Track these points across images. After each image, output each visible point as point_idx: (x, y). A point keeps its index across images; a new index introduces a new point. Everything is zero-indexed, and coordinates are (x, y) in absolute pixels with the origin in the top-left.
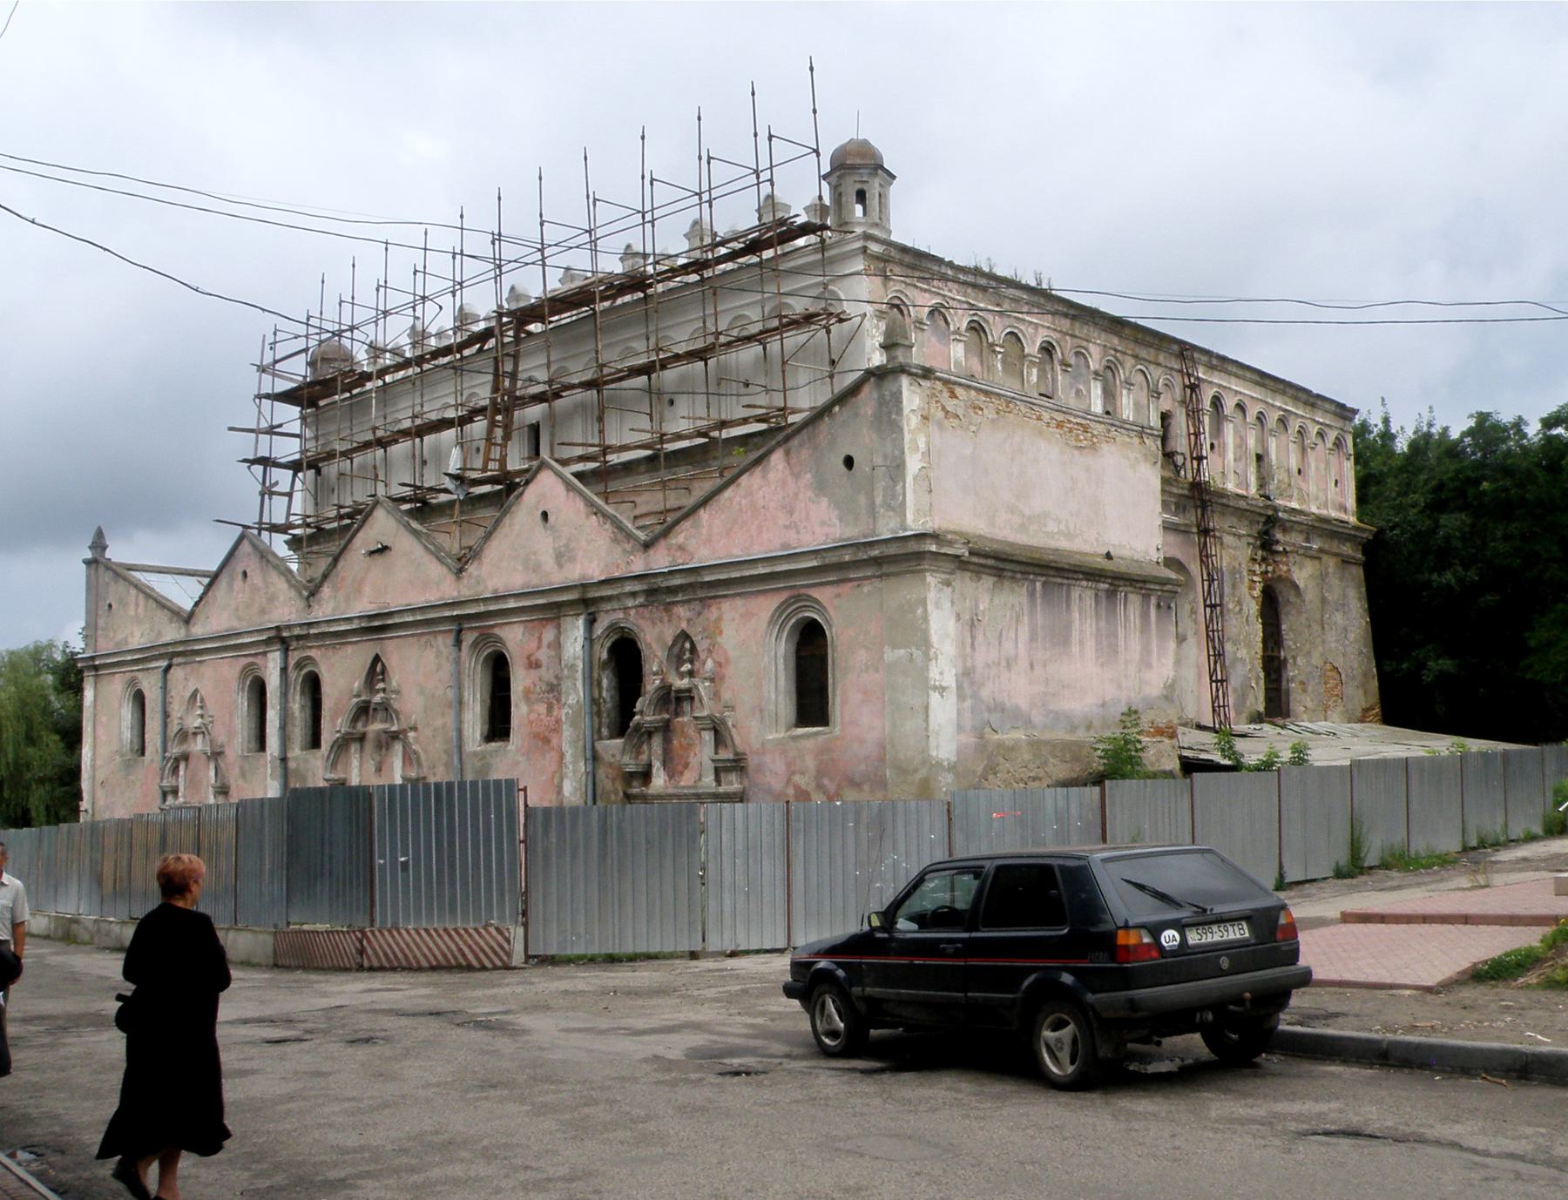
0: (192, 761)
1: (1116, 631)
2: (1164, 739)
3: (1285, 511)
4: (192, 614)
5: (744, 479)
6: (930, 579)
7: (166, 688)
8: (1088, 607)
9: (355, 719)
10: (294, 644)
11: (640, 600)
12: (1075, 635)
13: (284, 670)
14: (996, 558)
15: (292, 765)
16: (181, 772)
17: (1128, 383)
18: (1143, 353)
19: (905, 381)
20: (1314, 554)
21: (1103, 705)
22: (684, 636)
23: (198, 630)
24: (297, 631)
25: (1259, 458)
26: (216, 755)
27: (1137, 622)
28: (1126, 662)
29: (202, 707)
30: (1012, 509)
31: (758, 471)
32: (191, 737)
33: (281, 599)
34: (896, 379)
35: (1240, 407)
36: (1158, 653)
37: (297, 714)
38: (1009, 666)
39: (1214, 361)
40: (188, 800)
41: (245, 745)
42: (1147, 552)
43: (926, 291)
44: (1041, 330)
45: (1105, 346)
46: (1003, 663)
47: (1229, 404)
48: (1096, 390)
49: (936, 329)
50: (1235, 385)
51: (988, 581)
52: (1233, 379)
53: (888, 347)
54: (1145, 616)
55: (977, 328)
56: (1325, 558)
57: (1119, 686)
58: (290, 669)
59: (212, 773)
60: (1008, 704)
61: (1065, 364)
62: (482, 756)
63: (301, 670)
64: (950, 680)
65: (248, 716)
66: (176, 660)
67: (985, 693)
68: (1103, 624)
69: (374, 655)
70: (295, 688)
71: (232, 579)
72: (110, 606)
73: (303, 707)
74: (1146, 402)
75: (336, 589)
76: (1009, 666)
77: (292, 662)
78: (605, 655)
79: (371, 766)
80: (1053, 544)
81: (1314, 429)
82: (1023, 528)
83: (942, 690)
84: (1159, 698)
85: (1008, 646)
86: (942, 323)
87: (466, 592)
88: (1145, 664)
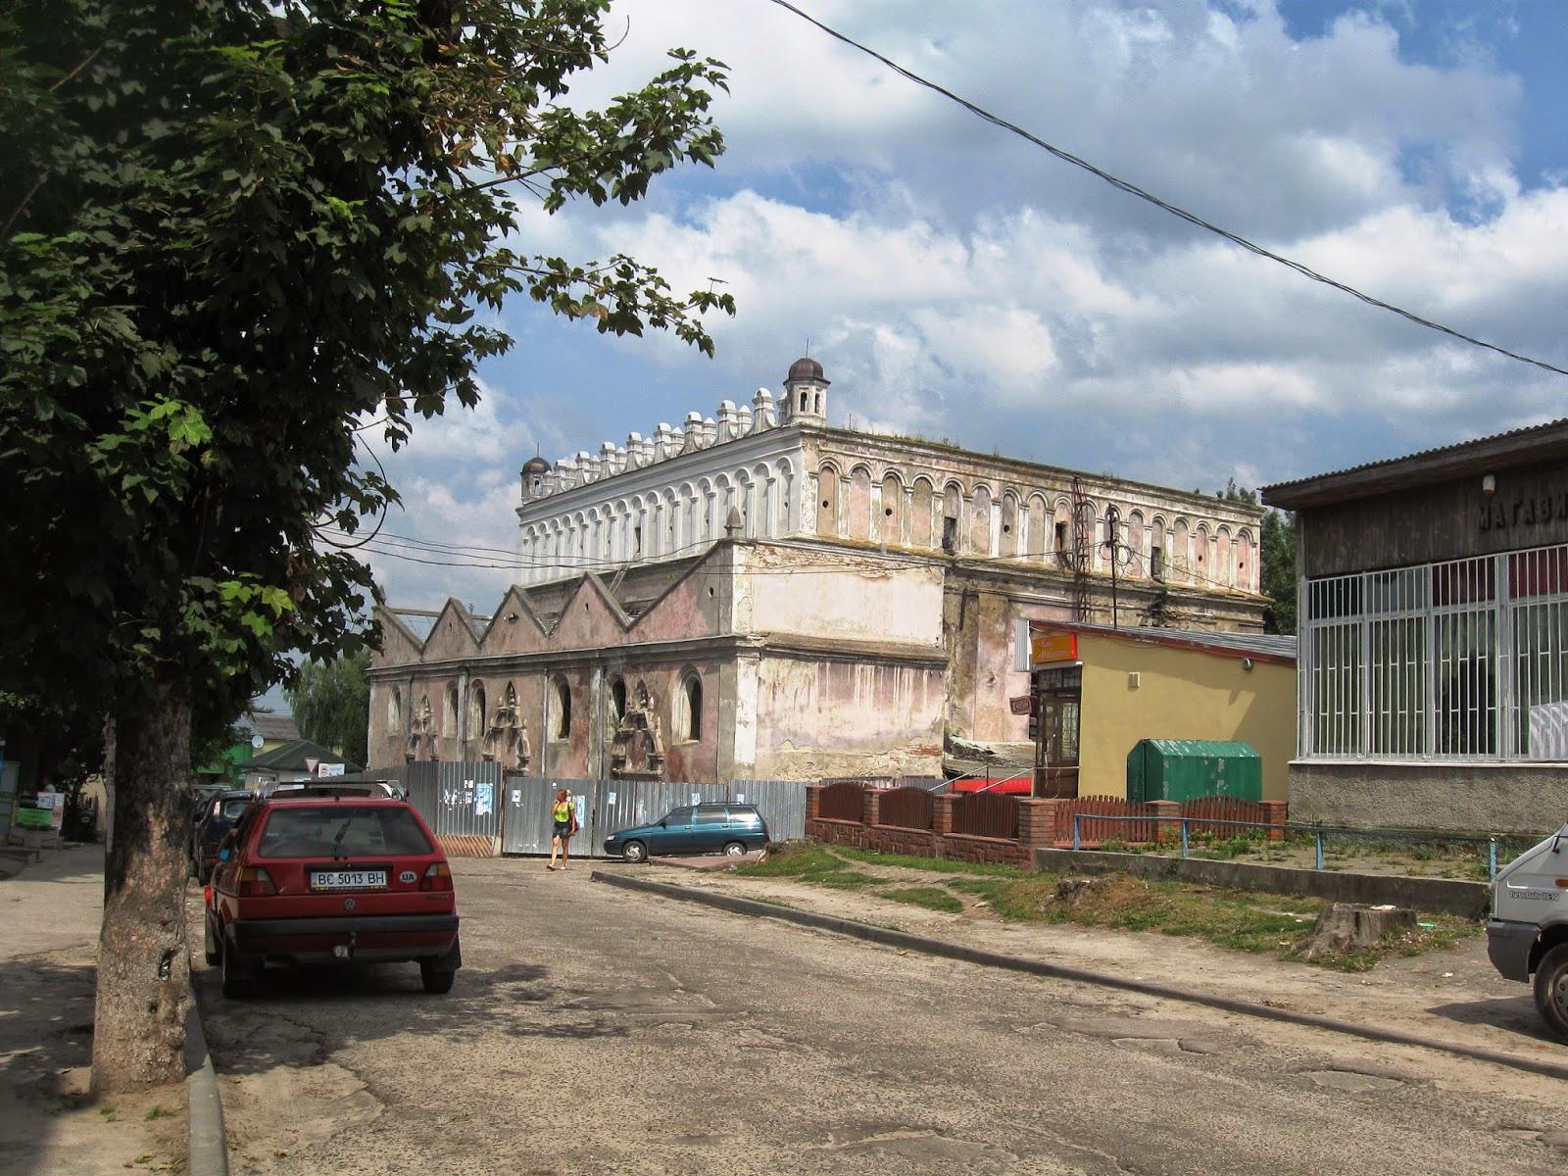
3: (1174, 590)
4: (424, 647)
5: (669, 596)
6: (740, 660)
10: (472, 671)
11: (625, 660)
13: (466, 687)
14: (792, 649)
15: (469, 745)
17: (1025, 506)
18: (1042, 483)
19: (735, 548)
20: (1209, 620)
21: (878, 734)
22: (642, 681)
23: (430, 657)
25: (1156, 551)
28: (899, 708)
30: (815, 618)
31: (675, 593)
34: (731, 547)
35: (1137, 513)
36: (929, 703)
38: (802, 710)
39: (1110, 484)
42: (927, 640)
44: (947, 474)
46: (798, 708)
47: (1125, 514)
48: (996, 512)
49: (859, 479)
50: (1130, 498)
51: (789, 662)
52: (1129, 495)
53: (729, 529)
54: (918, 681)
55: (892, 477)
56: (1220, 623)
57: (892, 723)
61: (967, 497)
62: (554, 746)
64: (753, 719)
66: (416, 676)
67: (782, 725)
71: (444, 628)
74: (1042, 516)
75: (493, 638)
78: (610, 691)
80: (847, 637)
81: (1214, 526)
82: (822, 628)
83: (746, 724)
85: (802, 699)
86: (864, 475)
87: (554, 648)
88: (916, 707)
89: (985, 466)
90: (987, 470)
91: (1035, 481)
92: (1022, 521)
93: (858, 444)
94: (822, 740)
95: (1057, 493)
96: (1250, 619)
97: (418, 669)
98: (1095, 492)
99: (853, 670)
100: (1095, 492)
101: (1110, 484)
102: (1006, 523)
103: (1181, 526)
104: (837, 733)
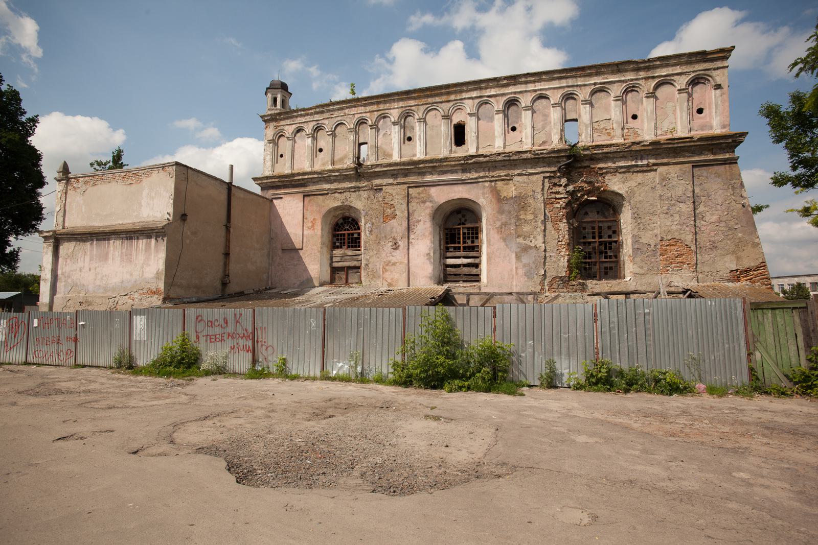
1: (132, 252)
2: (153, 296)
8: (118, 245)
12: (110, 256)
27: (143, 248)
38: (81, 270)
43: (292, 124)
45: (402, 107)
46: (78, 269)
47: (525, 100)
50: (531, 87)
57: (131, 275)
60: (79, 284)
68: (124, 250)
76: (81, 270)
83: (45, 280)
84: (153, 278)
89: (385, 102)
90: (388, 105)
91: (430, 100)
92: (418, 130)
93: (297, 117)
94: (91, 288)
95: (452, 103)
96: (712, 157)
98: (493, 92)
99: (109, 244)
100: (493, 92)
101: (505, 82)
102: (408, 135)
103: (602, 94)
104: (98, 283)
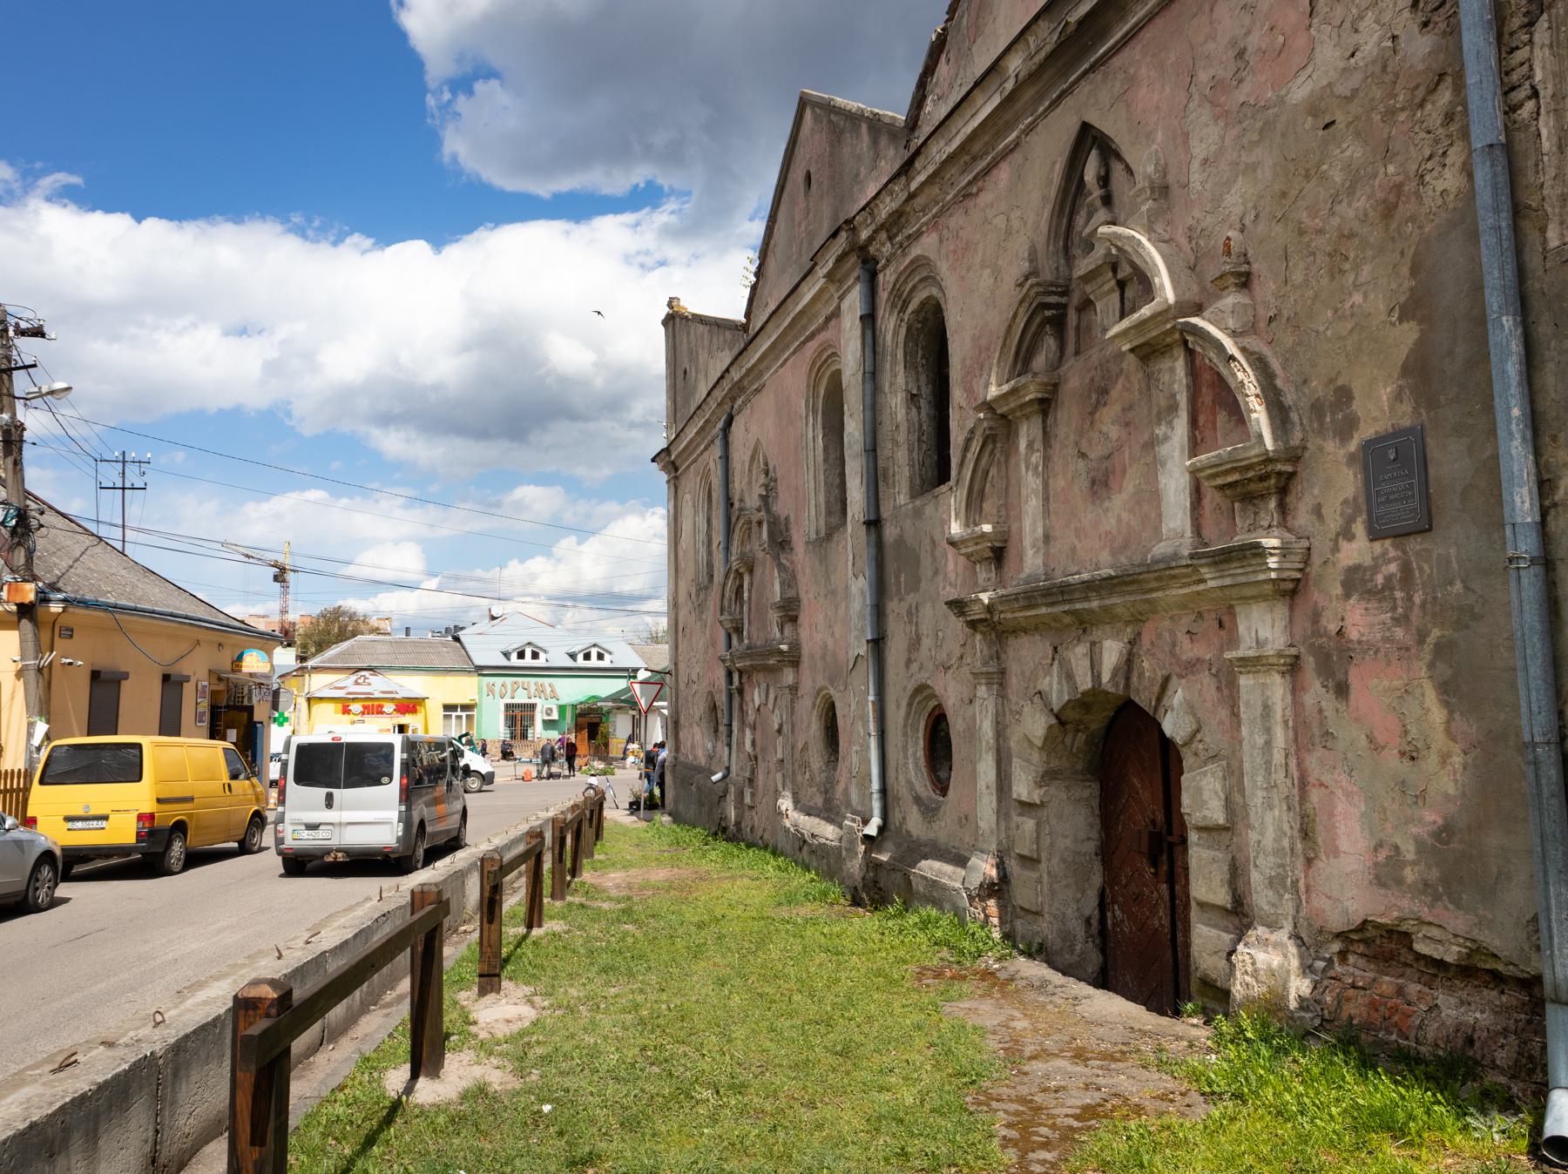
0: (758, 571)
7: (727, 458)
9: (1022, 360)
13: (869, 319)
15: (890, 532)
16: (746, 595)
24: (886, 208)
26: (780, 542)
29: (767, 473)
32: (755, 528)
33: (863, 171)
37: (901, 415)
40: (753, 641)
41: (822, 522)
58: (880, 313)
59: (777, 587)
63: (903, 309)
65: (825, 460)
69: (1077, 126)
70: (894, 362)
72: (685, 372)
73: (913, 398)
77: (883, 295)
79: (1071, 475)
97: (736, 375)
